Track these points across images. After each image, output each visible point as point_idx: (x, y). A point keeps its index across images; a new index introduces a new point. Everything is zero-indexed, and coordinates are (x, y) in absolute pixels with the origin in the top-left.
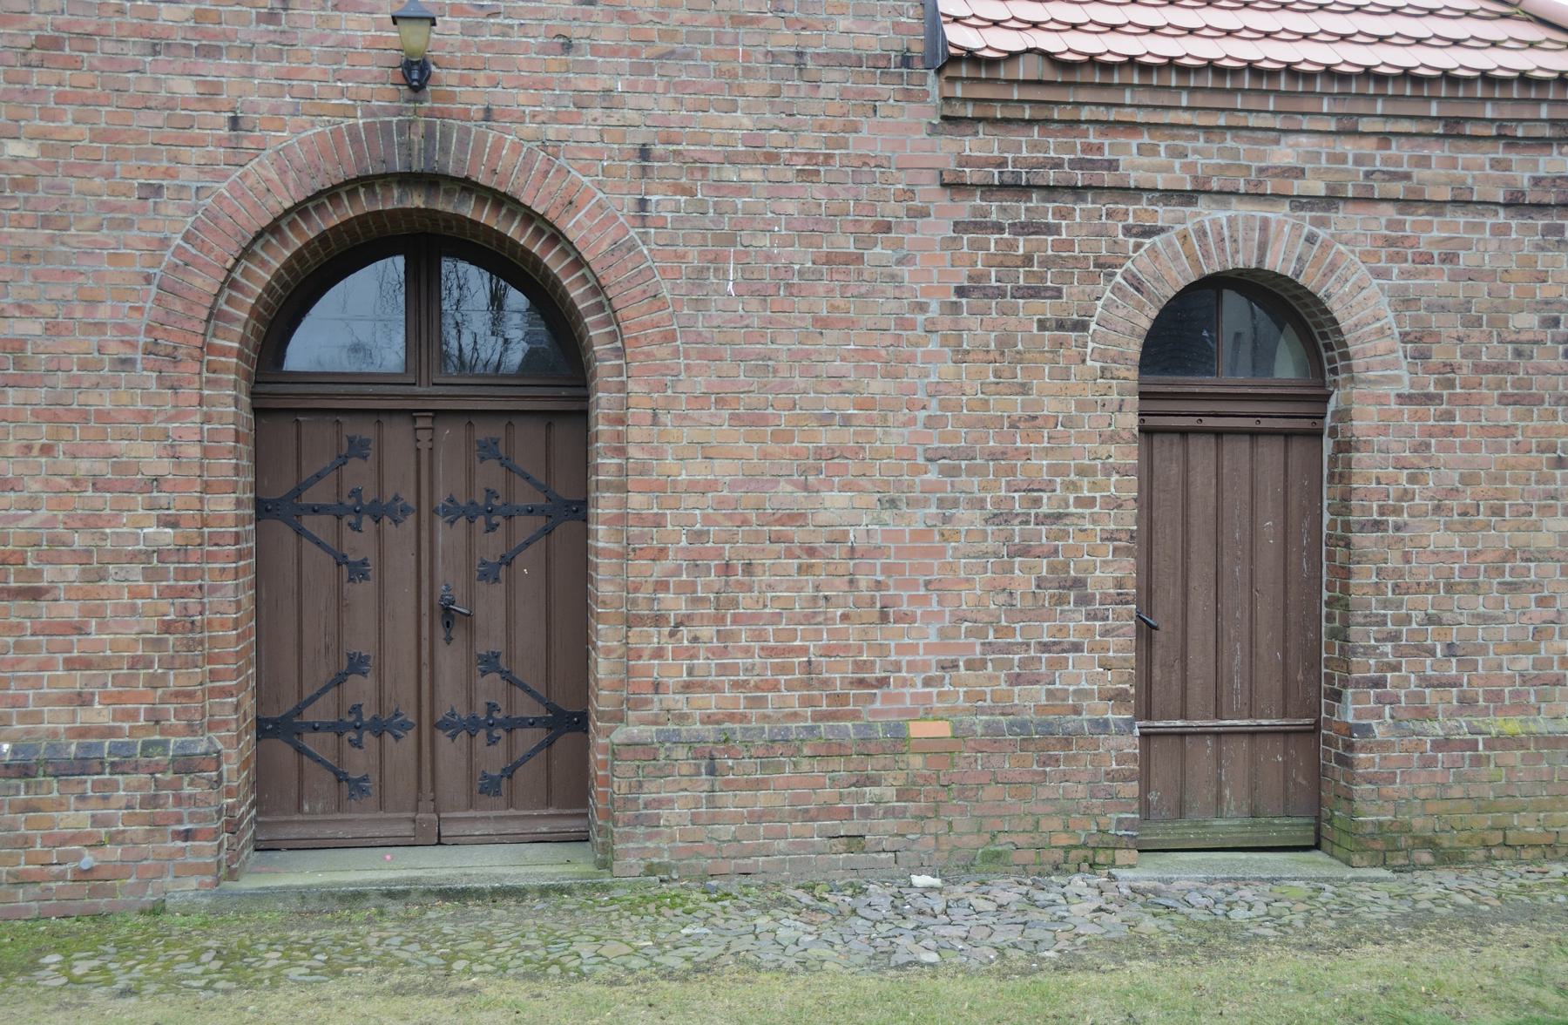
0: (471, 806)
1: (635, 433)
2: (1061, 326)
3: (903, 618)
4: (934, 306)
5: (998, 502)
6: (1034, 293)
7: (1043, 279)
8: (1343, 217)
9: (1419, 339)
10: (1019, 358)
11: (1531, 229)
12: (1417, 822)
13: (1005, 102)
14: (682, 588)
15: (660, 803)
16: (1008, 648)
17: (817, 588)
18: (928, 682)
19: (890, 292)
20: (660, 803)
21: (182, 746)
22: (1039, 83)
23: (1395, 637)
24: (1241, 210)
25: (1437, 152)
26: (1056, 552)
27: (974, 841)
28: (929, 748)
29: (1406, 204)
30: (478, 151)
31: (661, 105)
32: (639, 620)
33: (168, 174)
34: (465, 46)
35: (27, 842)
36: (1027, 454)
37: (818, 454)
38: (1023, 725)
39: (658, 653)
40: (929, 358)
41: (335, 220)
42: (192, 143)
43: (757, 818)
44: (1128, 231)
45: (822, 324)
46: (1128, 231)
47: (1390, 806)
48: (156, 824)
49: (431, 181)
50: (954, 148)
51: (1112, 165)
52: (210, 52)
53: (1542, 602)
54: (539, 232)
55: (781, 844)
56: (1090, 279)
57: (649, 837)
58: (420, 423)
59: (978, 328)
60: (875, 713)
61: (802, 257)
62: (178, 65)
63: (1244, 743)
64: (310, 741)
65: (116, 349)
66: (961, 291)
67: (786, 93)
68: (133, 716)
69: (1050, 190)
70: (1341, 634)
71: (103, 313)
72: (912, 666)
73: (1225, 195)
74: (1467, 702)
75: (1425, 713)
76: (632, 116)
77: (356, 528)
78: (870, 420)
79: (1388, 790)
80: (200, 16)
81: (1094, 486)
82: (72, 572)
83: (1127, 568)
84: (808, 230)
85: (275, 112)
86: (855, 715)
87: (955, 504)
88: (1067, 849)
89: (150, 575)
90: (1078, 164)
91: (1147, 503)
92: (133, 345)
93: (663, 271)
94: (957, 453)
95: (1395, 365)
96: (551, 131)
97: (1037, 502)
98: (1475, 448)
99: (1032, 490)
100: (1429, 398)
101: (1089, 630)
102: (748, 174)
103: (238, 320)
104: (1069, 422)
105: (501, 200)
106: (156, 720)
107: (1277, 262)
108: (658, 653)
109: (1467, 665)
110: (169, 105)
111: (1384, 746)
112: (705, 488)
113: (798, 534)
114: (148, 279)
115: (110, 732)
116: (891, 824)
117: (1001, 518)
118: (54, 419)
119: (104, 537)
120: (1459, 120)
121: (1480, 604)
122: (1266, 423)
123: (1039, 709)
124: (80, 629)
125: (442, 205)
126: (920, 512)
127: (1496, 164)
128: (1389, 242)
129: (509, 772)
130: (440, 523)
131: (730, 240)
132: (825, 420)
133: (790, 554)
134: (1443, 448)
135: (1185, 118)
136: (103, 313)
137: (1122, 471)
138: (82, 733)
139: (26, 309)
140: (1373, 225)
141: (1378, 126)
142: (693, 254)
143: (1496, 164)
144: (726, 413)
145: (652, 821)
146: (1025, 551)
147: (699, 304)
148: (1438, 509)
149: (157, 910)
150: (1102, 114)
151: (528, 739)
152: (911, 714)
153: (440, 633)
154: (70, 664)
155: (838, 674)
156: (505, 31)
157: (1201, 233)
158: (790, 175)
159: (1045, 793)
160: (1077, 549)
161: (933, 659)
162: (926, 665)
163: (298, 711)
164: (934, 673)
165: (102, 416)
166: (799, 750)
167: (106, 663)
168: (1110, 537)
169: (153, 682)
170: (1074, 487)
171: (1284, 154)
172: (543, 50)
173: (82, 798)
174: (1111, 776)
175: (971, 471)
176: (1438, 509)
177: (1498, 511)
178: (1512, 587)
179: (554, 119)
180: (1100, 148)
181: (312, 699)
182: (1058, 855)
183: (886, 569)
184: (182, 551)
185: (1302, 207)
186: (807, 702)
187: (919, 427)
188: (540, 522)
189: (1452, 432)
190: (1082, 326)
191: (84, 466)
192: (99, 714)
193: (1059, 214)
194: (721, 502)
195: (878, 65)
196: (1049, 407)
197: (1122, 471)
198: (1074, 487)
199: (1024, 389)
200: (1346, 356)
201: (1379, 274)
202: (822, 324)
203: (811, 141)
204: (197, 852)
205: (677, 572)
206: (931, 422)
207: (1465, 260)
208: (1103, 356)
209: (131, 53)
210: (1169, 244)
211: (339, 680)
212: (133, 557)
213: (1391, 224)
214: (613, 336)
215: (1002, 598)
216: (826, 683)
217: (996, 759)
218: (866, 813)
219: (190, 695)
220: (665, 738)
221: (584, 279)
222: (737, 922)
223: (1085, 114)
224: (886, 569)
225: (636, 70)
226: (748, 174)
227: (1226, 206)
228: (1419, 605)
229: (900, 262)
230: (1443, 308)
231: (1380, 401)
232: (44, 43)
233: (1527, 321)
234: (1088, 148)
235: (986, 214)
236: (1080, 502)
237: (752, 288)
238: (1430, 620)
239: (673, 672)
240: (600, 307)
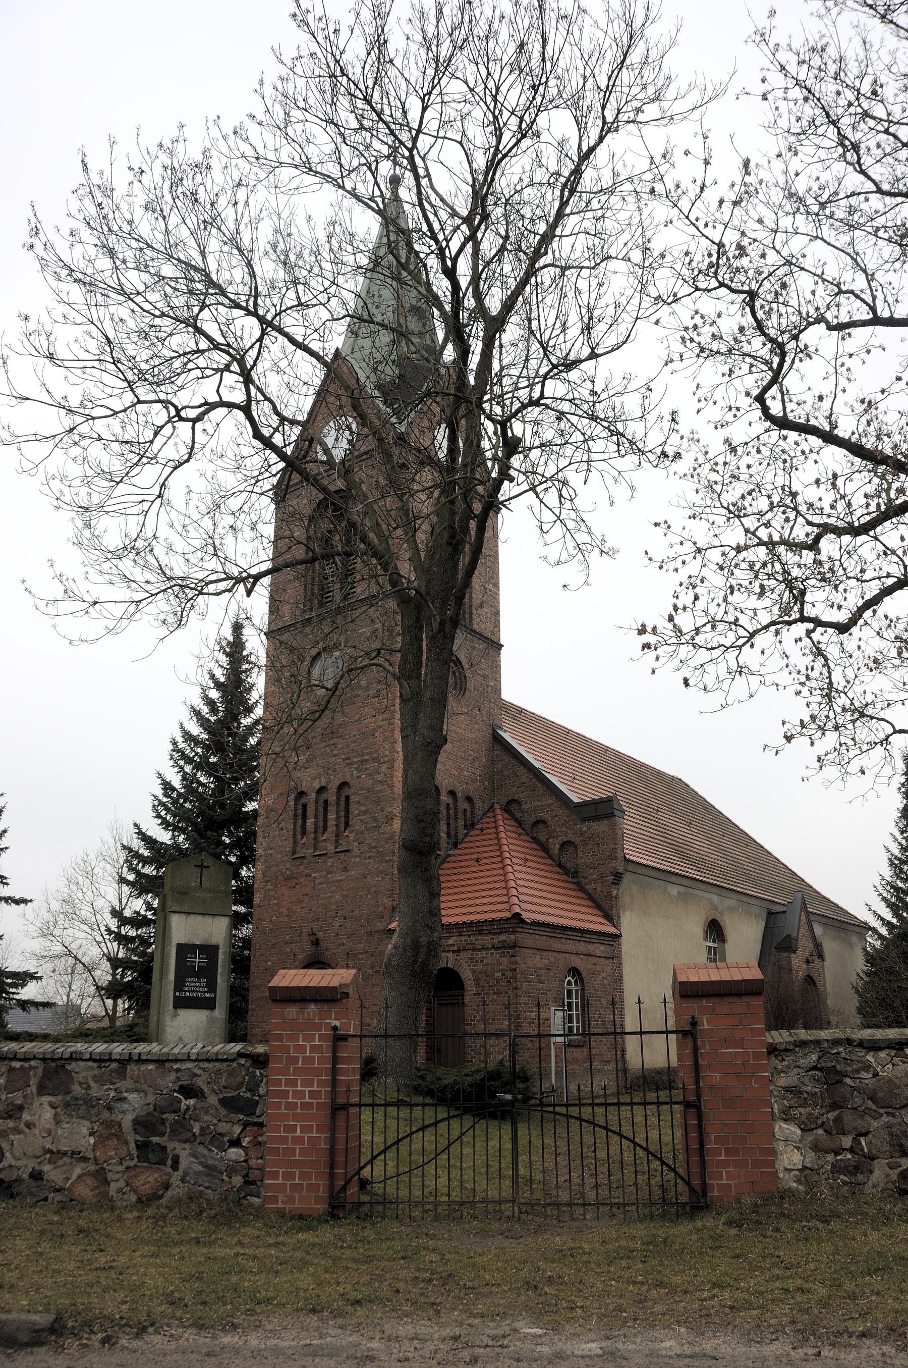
25: (479, 937)
29: (474, 950)
61: (371, 972)
107: (449, 965)
171: (451, 941)
203: (373, 949)
233: (498, 974)
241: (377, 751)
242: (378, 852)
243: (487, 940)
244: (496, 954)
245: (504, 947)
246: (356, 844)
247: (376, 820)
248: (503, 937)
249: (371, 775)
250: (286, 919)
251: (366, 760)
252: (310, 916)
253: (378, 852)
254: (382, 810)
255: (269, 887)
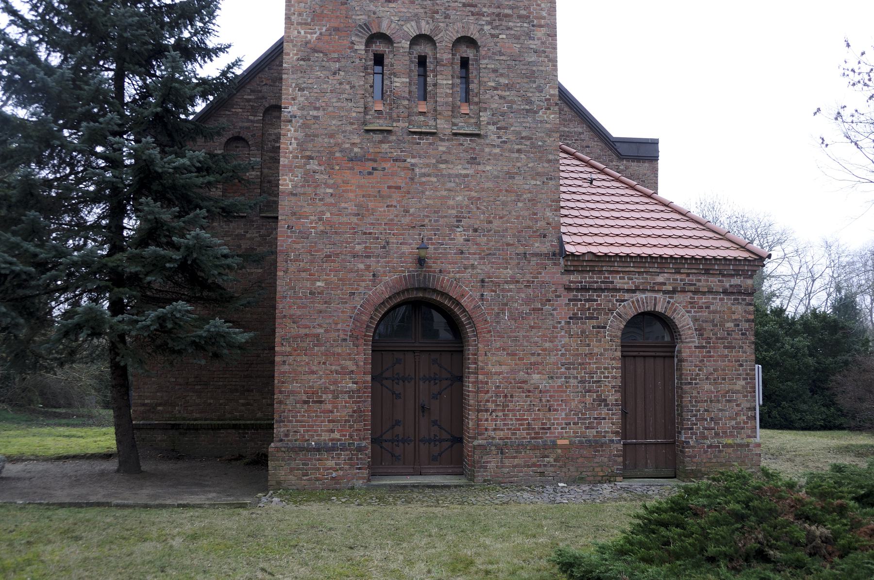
0: (429, 464)
1: (480, 358)
2: (599, 327)
3: (556, 410)
4: (563, 322)
5: (581, 377)
6: (592, 318)
7: (593, 314)
8: (679, 297)
9: (700, 330)
10: (587, 336)
11: (730, 299)
12: (703, 469)
13: (582, 266)
14: (493, 402)
15: (487, 462)
16: (585, 419)
17: (531, 402)
18: (562, 429)
19: (551, 318)
20: (487, 462)
21: (358, 444)
22: (591, 261)
23: (696, 416)
24: (649, 294)
26: (598, 391)
27: (576, 474)
28: (562, 447)
29: (696, 292)
30: (438, 281)
31: (487, 268)
32: (482, 411)
33: (357, 289)
34: (435, 253)
35: (319, 469)
36: (590, 364)
37: (531, 364)
38: (589, 441)
39: (487, 420)
40: (562, 337)
41: (399, 300)
42: (363, 281)
43: (515, 467)
44: (617, 301)
45: (532, 327)
46: (617, 301)
47: (695, 465)
48: (352, 465)
49: (425, 289)
50: (568, 278)
51: (612, 282)
52: (368, 257)
53: (737, 405)
54: (453, 303)
55: (521, 474)
56: (607, 314)
57: (485, 472)
58: (416, 354)
59: (575, 329)
60: (547, 437)
62: (360, 261)
63: (654, 447)
64: (384, 445)
65: (342, 336)
66: (570, 318)
67: (521, 264)
68: (345, 435)
69: (595, 290)
70: (680, 415)
71: (339, 326)
72: (558, 424)
73: (644, 291)
74: (717, 434)
75: (705, 438)
76: (479, 271)
77: (398, 384)
78: (545, 354)
79: (695, 460)
80: (366, 248)
81: (609, 373)
82: (330, 396)
83: (618, 396)
84: (528, 301)
85: (384, 272)
86: (541, 438)
87: (570, 378)
88: (602, 476)
89: (350, 397)
90: (602, 282)
91: (624, 377)
92: (347, 335)
93: (488, 313)
94: (570, 363)
95: (694, 337)
96: (458, 276)
97: (593, 377)
98: (717, 361)
99: (591, 374)
100: (704, 347)
101: (608, 414)
102: (511, 287)
103: (372, 327)
104: (601, 354)
105: (444, 294)
106: (351, 436)
107: (659, 309)
108: (487, 420)
109: (717, 424)
110: (357, 271)
111: (693, 447)
112: (500, 373)
113: (525, 386)
114: (351, 317)
115: (339, 440)
116: (552, 469)
117: (583, 382)
118: (327, 355)
119: (338, 387)
120: (708, 269)
121: (720, 406)
122: (658, 354)
123: (594, 436)
124: (332, 412)
125: (427, 296)
126: (560, 380)
127: (719, 281)
128: (691, 303)
129: (440, 455)
130: (421, 383)
131: (506, 305)
132: (533, 354)
133: (523, 392)
134: (707, 361)
135: (632, 269)
136: (339, 326)
137: (617, 368)
138: (332, 440)
139: (320, 326)
140: (686, 298)
141: (686, 271)
142: (496, 308)
143: (719, 281)
144: (505, 353)
145: (485, 467)
146: (589, 391)
147: (498, 323)
148: (707, 379)
149: (352, 488)
150: (609, 269)
151: (446, 445)
152: (558, 437)
153: (421, 414)
154: (329, 421)
155: (537, 426)
156: (445, 249)
157: (638, 301)
158: (523, 286)
159: (596, 460)
160: (604, 390)
161: (564, 422)
162: (561, 424)
163: (381, 436)
164: (564, 426)
165: (338, 354)
166: (526, 447)
167: (338, 421)
168: (613, 387)
169: (351, 427)
170: (604, 373)
171: (660, 279)
172: (455, 254)
173: (333, 457)
174: (615, 456)
175: (574, 369)
176: (707, 379)
177: (724, 379)
178: (729, 401)
179: (458, 272)
180: (609, 278)
181: (385, 433)
182: (600, 478)
183: (551, 396)
184: (358, 391)
185: (666, 294)
186: (528, 434)
187: (559, 356)
188: (449, 382)
189: (710, 357)
190: (605, 327)
191: (334, 368)
192: (336, 435)
193: (598, 296)
194: (504, 378)
195: (546, 255)
196: (596, 350)
197: (617, 368)
198: (604, 373)
199: (589, 345)
200: (680, 335)
201: (688, 312)
202: (532, 327)
203: (528, 277)
204: (363, 473)
205: (492, 397)
206: (562, 355)
207: (712, 308)
208: (610, 336)
209: (348, 258)
210: (629, 304)
211: (393, 427)
212: (346, 392)
213: (691, 298)
214: (473, 331)
215: (583, 405)
216: (534, 429)
217: (581, 451)
218: (545, 466)
219: (360, 430)
220: (489, 444)
221: (465, 316)
222: (511, 494)
223: (604, 269)
224: (551, 396)
225: (481, 258)
226: (511, 287)
227: (644, 293)
228: (702, 407)
229: (553, 310)
230: (706, 321)
231: (690, 348)
232: (327, 256)
234: (605, 278)
235: (577, 296)
236: (604, 377)
237: (511, 318)
238: (706, 411)
239: (491, 425)
240: (470, 323)
241: (526, 8)
242: (533, 145)
243: (714, 282)
244: (728, 301)
245: (740, 293)
246: (492, 128)
247: (529, 102)
248: (736, 281)
249: (517, 38)
250: (355, 220)
251: (507, 16)
252: (406, 220)
253: (533, 145)
254: (540, 89)
255: (313, 165)
